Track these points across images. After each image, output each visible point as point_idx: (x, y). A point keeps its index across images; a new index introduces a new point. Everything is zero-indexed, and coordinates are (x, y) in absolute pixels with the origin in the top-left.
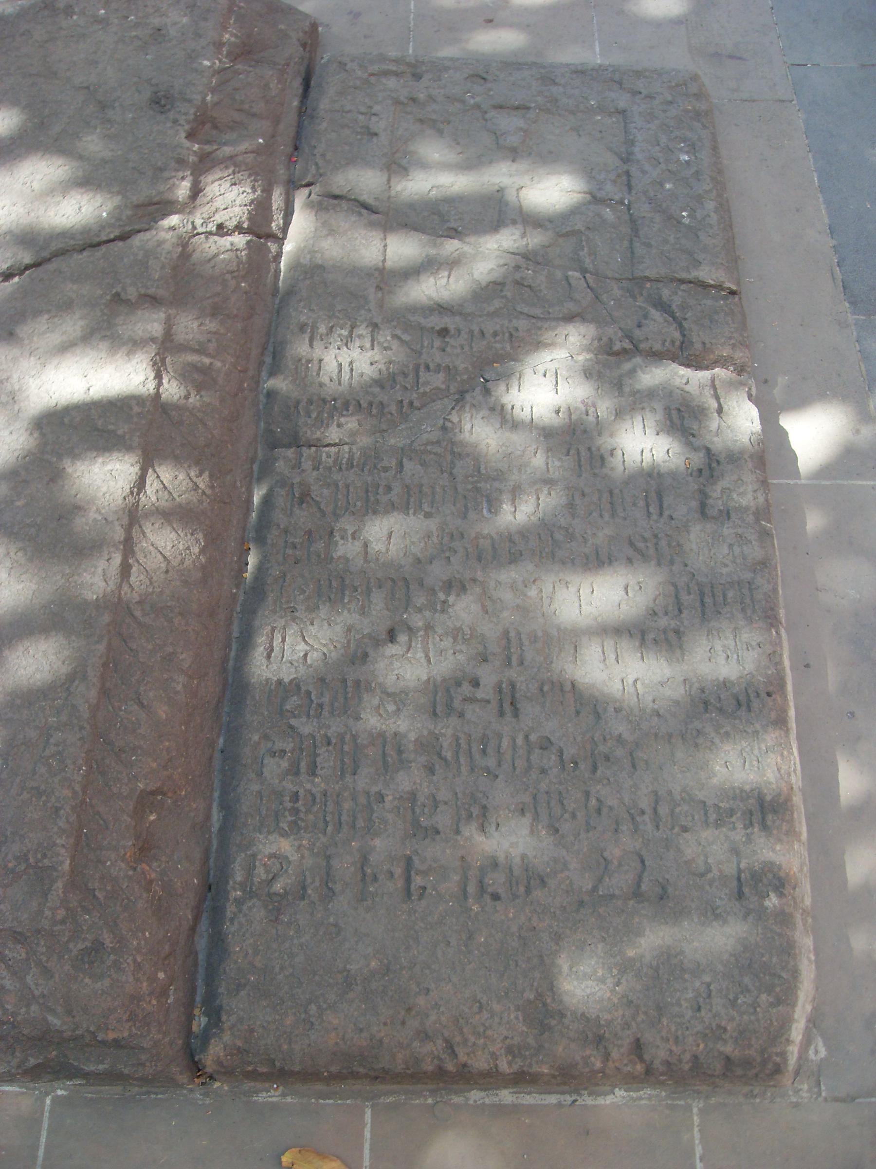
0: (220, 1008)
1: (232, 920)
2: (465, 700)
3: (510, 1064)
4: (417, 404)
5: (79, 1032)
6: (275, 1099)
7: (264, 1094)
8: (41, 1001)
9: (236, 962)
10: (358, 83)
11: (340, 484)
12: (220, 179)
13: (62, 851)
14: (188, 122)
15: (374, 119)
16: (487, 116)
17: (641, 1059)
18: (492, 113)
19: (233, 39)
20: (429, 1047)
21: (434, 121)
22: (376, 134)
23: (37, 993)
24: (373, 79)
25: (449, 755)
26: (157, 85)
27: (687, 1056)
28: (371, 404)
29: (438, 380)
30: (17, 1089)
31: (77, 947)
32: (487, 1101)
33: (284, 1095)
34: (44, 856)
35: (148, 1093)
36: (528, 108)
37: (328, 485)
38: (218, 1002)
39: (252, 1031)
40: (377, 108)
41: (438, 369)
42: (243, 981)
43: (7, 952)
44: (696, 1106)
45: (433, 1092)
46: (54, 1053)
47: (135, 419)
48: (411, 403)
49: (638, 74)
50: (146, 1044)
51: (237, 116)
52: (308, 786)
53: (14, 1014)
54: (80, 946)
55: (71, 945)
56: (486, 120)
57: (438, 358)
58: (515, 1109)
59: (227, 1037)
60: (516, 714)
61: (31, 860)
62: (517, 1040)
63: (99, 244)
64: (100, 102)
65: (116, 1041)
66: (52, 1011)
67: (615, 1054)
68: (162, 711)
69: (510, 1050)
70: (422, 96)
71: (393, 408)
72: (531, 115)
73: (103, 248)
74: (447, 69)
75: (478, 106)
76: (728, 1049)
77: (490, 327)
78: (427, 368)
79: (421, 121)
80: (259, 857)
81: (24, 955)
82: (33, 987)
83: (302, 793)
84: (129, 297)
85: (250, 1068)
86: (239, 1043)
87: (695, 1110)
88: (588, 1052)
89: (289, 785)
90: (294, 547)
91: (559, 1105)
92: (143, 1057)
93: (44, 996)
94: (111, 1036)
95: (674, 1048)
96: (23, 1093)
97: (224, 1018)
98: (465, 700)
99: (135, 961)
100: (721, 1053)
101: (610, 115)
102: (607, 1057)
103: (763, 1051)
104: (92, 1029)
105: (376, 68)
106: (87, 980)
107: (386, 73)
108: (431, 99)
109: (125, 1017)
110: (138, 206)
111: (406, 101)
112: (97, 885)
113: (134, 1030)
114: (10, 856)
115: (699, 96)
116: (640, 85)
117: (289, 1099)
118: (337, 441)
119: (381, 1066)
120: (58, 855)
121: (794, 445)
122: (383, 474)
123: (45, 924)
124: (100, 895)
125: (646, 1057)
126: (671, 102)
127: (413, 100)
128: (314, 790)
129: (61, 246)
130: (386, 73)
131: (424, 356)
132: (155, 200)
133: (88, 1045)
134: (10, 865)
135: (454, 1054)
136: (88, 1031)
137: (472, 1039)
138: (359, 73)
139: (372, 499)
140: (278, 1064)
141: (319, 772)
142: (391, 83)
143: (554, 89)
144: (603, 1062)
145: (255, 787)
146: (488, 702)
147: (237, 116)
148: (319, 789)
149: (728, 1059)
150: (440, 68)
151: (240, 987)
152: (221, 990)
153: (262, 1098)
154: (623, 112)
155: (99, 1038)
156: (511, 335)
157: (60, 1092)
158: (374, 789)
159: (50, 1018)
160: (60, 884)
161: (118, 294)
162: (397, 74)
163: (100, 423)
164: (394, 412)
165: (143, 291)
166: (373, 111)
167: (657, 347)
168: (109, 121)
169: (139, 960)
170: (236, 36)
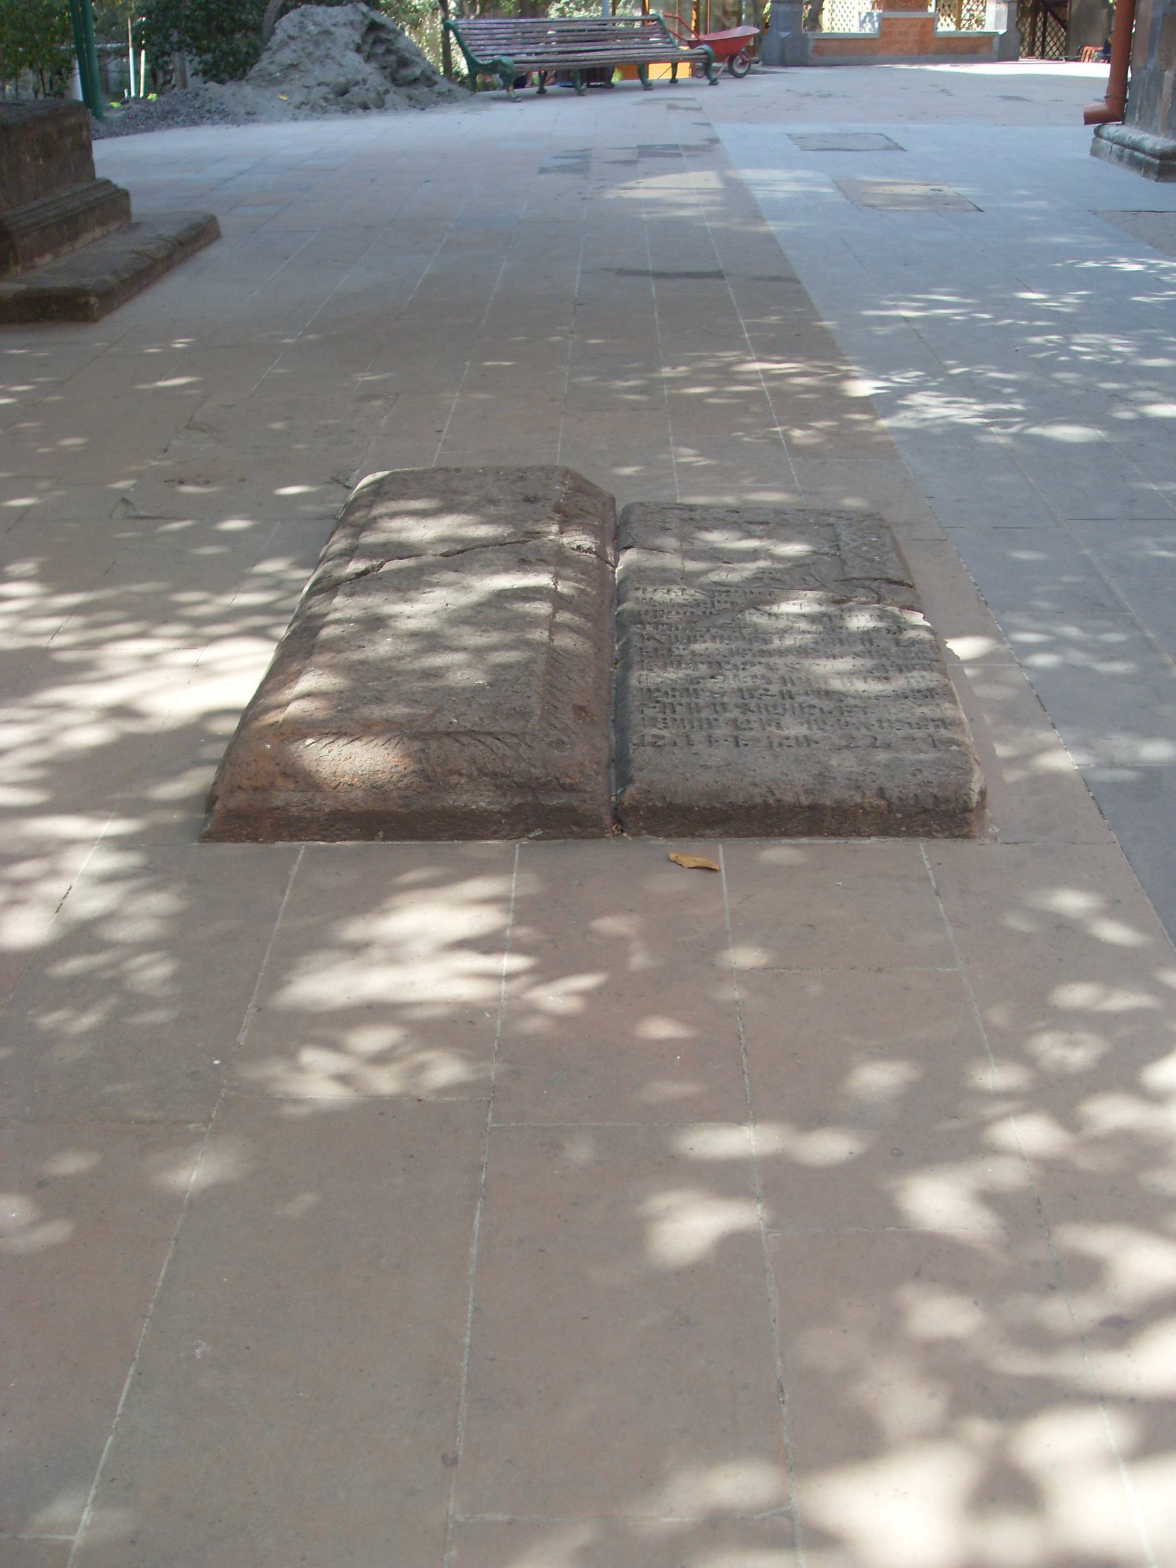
3: (806, 798)
5: (549, 778)
8: (528, 761)
12: (576, 530)
17: (884, 798)
20: (758, 790)
23: (525, 757)
25: (755, 709)
27: (911, 795)
29: (728, 605)
32: (793, 842)
36: (769, 523)
41: (726, 602)
44: (921, 846)
45: (758, 840)
46: (530, 798)
50: (588, 789)
53: (510, 769)
57: (726, 599)
58: (810, 844)
62: (810, 786)
65: (571, 785)
66: (535, 766)
67: (868, 794)
69: (806, 792)
70: (698, 518)
72: (771, 525)
76: (935, 791)
82: (523, 754)
85: (650, 804)
86: (645, 787)
87: (921, 846)
88: (852, 793)
91: (838, 843)
92: (587, 796)
93: (529, 758)
94: (568, 781)
95: (903, 791)
100: (931, 793)
101: (823, 526)
102: (863, 796)
103: (956, 793)
104: (558, 775)
105: (662, 506)
108: (704, 519)
116: (842, 515)
119: (730, 800)
121: (956, 653)
125: (887, 796)
133: (555, 789)
135: (773, 793)
136: (555, 777)
137: (783, 786)
140: (668, 799)
143: (785, 516)
144: (862, 798)
149: (935, 797)
153: (653, 842)
154: (832, 525)
158: (711, 717)
159: (532, 770)
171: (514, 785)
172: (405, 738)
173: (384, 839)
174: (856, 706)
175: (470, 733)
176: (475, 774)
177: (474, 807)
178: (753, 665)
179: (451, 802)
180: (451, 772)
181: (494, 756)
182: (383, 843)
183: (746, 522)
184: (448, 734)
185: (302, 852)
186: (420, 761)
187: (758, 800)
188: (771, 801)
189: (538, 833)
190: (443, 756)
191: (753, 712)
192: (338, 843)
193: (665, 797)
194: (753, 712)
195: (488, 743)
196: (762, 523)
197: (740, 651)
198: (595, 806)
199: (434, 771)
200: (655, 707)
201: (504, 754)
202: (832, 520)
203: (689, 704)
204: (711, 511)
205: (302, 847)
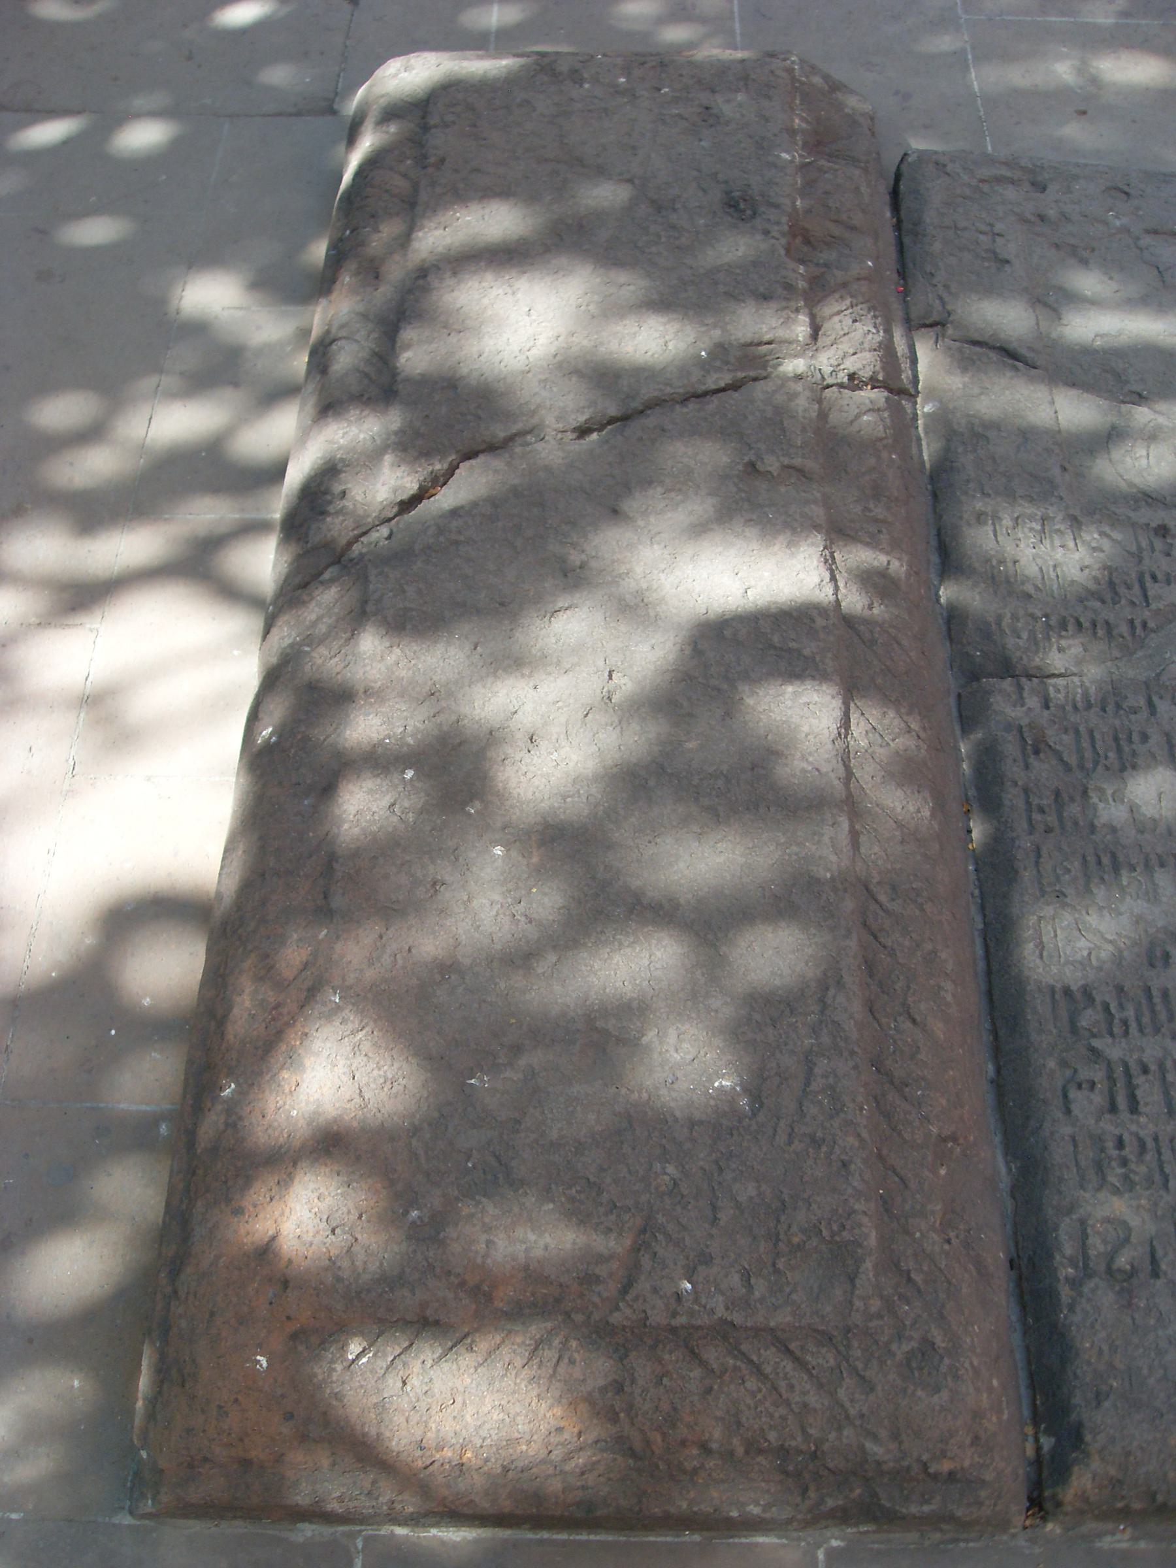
0: (1080, 1425)
1: (1071, 1308)
4: (1151, 624)
5: (905, 1463)
6: (1124, 1545)
7: (1108, 1538)
8: (858, 1422)
9: (1089, 1363)
10: (968, 192)
11: (1082, 729)
12: (839, 313)
13: (865, 1220)
14: (783, 234)
16: (1141, 243)
18: (1147, 240)
19: (804, 125)
21: (1074, 247)
22: (1008, 262)
23: (852, 1412)
24: (985, 188)
26: (726, 182)
30: (777, 1541)
31: (901, 1349)
33: (1134, 1539)
34: (843, 1227)
35: (955, 1540)
37: (1066, 731)
38: (1074, 1416)
39: (1128, 1454)
40: (999, 227)
42: (1104, 1388)
43: (809, 1358)
46: (858, 1491)
47: (822, 635)
48: (1144, 625)
50: (989, 1476)
51: (836, 230)
52: (1134, 1128)
54: (906, 1347)
55: (894, 1347)
56: (1141, 249)
59: (1096, 1464)
61: (825, 1233)
63: (706, 394)
64: (653, 202)
66: (875, 1438)
68: (938, 1028)
70: (1052, 213)
71: (1124, 629)
73: (714, 403)
74: (1076, 177)
75: (1126, 230)
78: (1154, 578)
79: (1057, 246)
80: (1090, 1222)
81: (832, 1362)
82: (847, 1404)
84: (769, 469)
86: (1112, 1471)
89: (1108, 1126)
90: (1042, 810)
93: (862, 1416)
94: (946, 1466)
96: (784, 1546)
97: (1088, 1438)
99: (971, 1364)
104: (925, 1457)
105: (985, 172)
106: (919, 1393)
107: (999, 180)
108: (1065, 217)
109: (968, 1441)
111: (1033, 219)
112: (911, 1265)
113: (977, 1459)
114: (795, 1229)
117: (1142, 1545)
118: (1063, 671)
120: (860, 1225)
122: (1133, 717)
123: (857, 1318)
124: (918, 1278)
127: (1042, 218)
128: (1142, 1133)
129: (656, 394)
130: (999, 180)
131: (1146, 561)
134: (796, 1240)
136: (919, 1460)
138: (965, 178)
139: (1126, 749)
141: (1142, 1109)
142: (1010, 193)
145: (1067, 1130)
147: (836, 230)
148: (1147, 1131)
151: (1099, 1398)
152: (1077, 1400)
153: (1106, 1543)
155: (931, 1470)
157: (835, 1543)
159: (869, 1445)
160: (868, 1264)
162: (1012, 182)
163: (776, 639)
164: (1125, 634)
165: (786, 461)
166: (996, 230)
168: (673, 227)
169: (976, 1363)
170: (808, 122)
175: (724, 1331)
176: (740, 1451)
177: (734, 1514)
179: (684, 1505)
181: (782, 1411)
183: (1148, 232)
186: (614, 1419)
190: (665, 1406)
193: (1155, 1493)
195: (768, 1369)
198: (998, 1508)
199: (648, 1443)
201: (805, 1405)
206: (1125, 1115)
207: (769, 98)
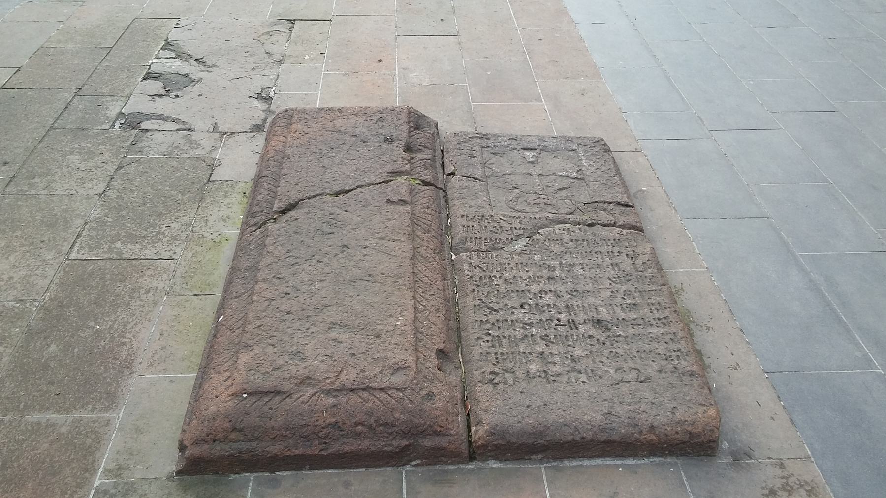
2: (556, 325)
15: (474, 152)
24: (470, 139)
28: (496, 239)
29: (521, 232)
49: (578, 138)
60: (577, 329)
72: (538, 151)
74: (499, 136)
76: (689, 429)
77: (537, 216)
78: (516, 228)
83: (498, 352)
98: (556, 325)
108: (495, 146)
110: (388, 173)
115: (605, 145)
116: (580, 142)
126: (594, 147)
132: (395, 171)
146: (565, 326)
149: (690, 433)
150: (496, 136)
156: (547, 219)
161: (388, 200)
165: (400, 198)
167: (606, 222)
171: (401, 433)
172: (322, 395)
173: (310, 469)
174: (619, 336)
178: (546, 293)
180: (357, 424)
182: (309, 472)
184: (352, 390)
185: (251, 484)
187: (570, 438)
188: (578, 438)
189: (418, 462)
191: (552, 343)
192: (277, 473)
194: (552, 343)
196: (531, 150)
197: (536, 279)
199: (344, 424)
200: (488, 341)
202: (575, 147)
203: (510, 336)
204: (500, 139)
205: (251, 476)
206: (497, 348)
207: (400, 114)
